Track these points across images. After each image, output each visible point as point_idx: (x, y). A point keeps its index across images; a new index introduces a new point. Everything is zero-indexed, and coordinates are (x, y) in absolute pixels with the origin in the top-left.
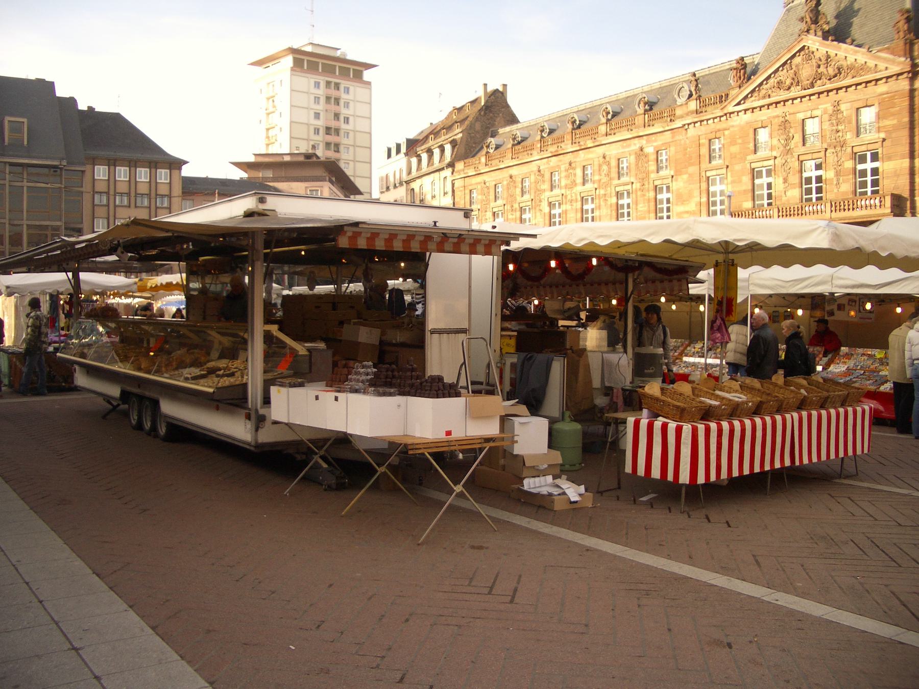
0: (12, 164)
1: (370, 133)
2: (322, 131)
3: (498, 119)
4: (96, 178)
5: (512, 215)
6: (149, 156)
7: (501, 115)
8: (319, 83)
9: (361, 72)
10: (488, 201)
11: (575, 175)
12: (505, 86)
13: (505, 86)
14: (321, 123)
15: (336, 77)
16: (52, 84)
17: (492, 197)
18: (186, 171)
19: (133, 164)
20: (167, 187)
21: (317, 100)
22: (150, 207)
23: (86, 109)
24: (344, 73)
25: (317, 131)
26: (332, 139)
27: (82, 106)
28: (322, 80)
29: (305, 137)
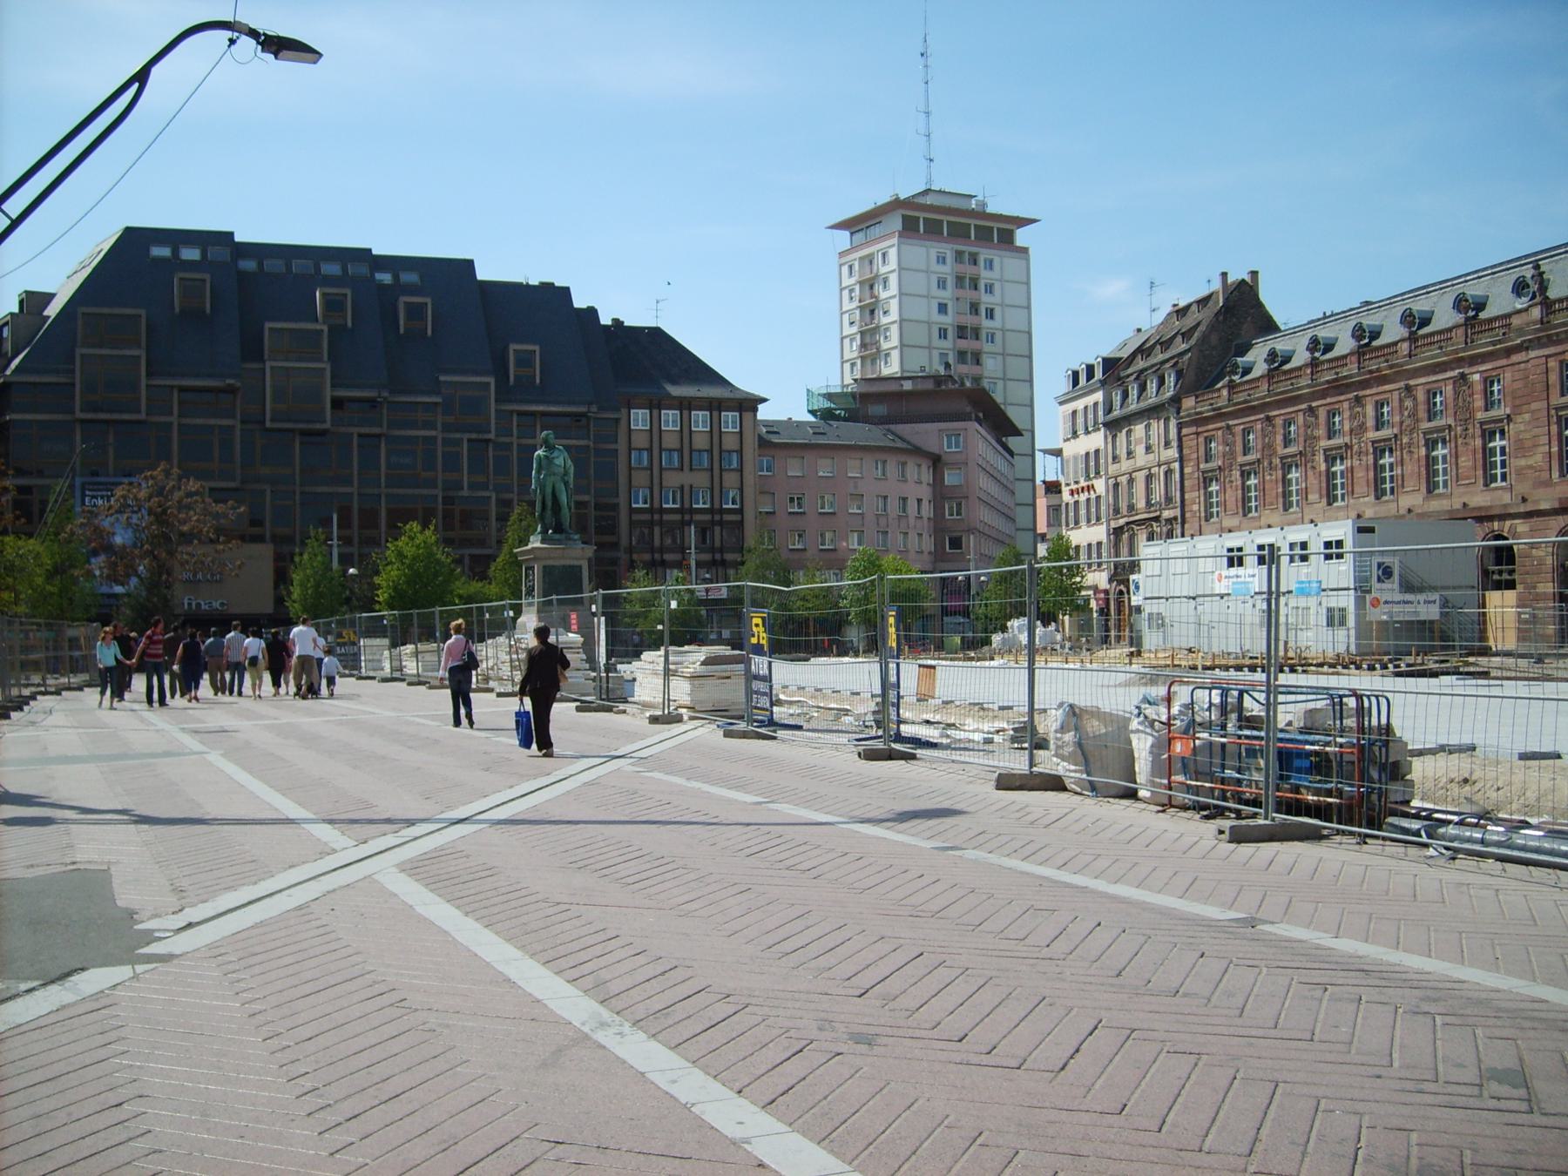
0: (520, 414)
1: (1029, 333)
3: (1245, 326)
4: (632, 427)
5: (1271, 475)
7: (1249, 319)
10: (1232, 453)
11: (1364, 417)
12: (1254, 274)
13: (1254, 274)
14: (948, 320)
16: (567, 289)
17: (1239, 448)
18: (764, 412)
21: (942, 284)
22: (712, 469)
23: (610, 323)
24: (984, 235)
25: (943, 334)
27: (605, 319)
28: (948, 250)
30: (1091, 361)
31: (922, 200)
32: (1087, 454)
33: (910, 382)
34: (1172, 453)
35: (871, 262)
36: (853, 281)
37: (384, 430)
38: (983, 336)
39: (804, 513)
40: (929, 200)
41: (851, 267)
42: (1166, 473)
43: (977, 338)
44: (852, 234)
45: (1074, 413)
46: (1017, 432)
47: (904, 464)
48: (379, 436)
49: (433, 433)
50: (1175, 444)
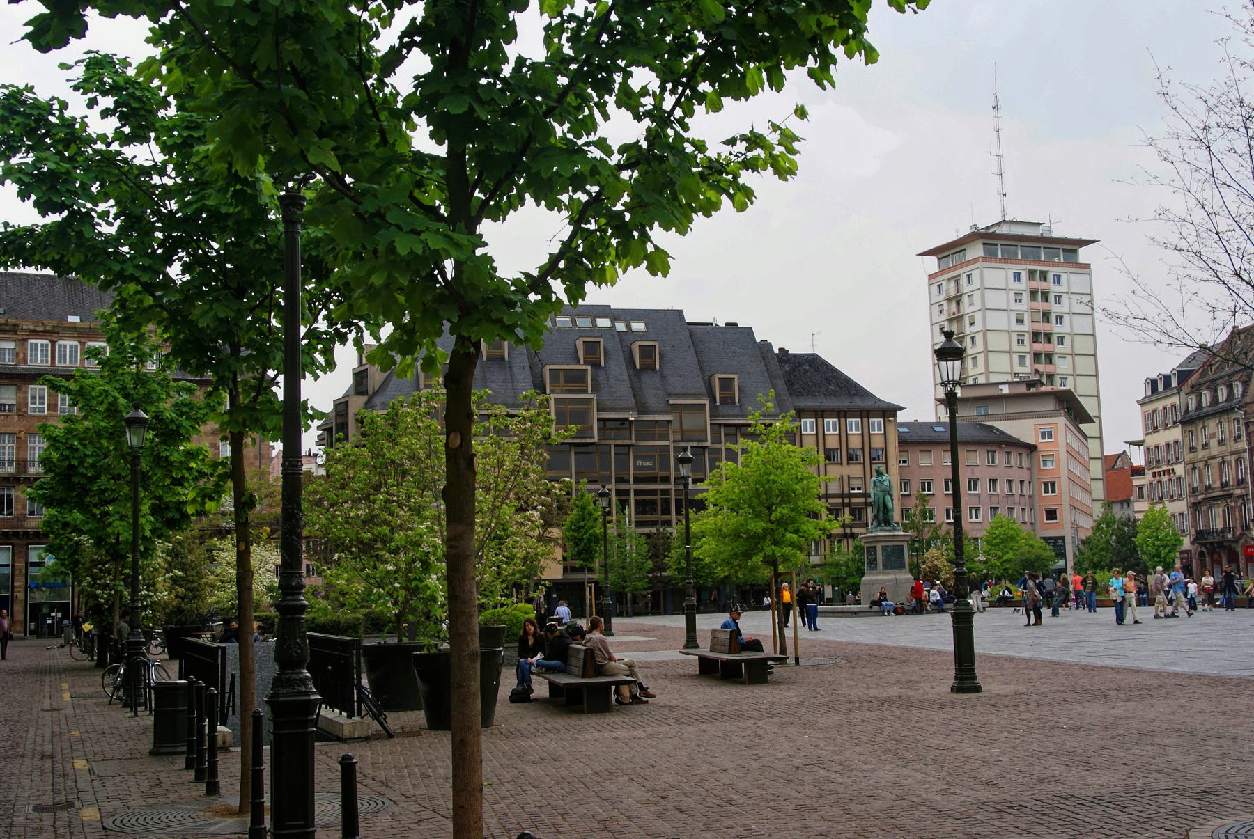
0: (726, 425)
1: (1093, 335)
2: (1027, 339)
6: (859, 403)
8: (1019, 274)
9: (1075, 251)
14: (1026, 327)
15: (1043, 263)
18: (901, 417)
19: (842, 414)
20: (881, 439)
26: (1040, 347)
28: (1024, 269)
29: (1008, 349)
30: (1167, 372)
31: (998, 230)
32: (1168, 444)
33: (1007, 386)
34: (1243, 445)
35: (957, 282)
36: (942, 297)
37: (633, 442)
38: (1054, 338)
39: (933, 495)
40: (1005, 230)
41: (939, 286)
42: (1237, 461)
43: (1049, 342)
44: (939, 259)
45: (1154, 411)
46: (1089, 420)
47: (1008, 453)
48: (629, 446)
49: (666, 443)
50: (1244, 438)
